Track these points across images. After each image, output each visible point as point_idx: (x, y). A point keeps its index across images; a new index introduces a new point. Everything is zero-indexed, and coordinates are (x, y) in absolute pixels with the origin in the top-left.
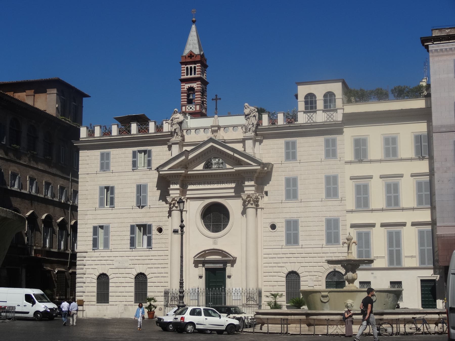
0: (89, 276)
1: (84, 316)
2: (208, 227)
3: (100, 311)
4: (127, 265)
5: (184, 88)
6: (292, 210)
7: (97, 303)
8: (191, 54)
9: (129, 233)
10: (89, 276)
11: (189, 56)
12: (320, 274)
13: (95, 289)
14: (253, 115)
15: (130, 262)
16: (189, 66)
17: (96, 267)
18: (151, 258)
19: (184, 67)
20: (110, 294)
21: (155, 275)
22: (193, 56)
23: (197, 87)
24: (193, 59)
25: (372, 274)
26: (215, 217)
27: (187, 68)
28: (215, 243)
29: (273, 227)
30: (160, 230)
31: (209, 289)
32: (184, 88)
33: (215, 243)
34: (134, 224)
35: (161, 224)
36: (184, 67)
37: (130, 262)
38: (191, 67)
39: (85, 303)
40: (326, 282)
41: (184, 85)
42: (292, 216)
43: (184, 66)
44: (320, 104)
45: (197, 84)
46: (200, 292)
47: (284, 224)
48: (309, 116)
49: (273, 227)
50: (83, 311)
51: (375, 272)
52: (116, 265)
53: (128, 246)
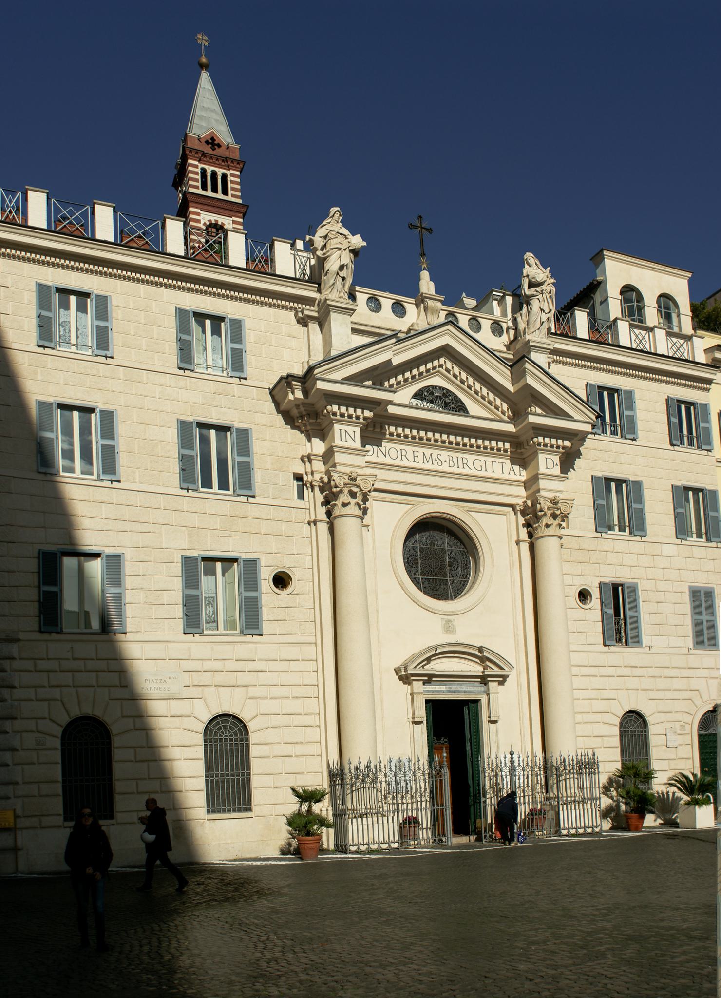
1: (22, 867)
8: (213, 139)
9: (177, 583)
11: (207, 142)
15: (186, 679)
16: (209, 169)
19: (197, 167)
20: (119, 786)
21: (276, 721)
22: (219, 146)
24: (218, 152)
26: (440, 556)
27: (204, 171)
28: (449, 628)
30: (281, 580)
33: (449, 628)
34: (195, 554)
35: (286, 564)
36: (197, 167)
37: (186, 679)
38: (214, 174)
40: (700, 736)
43: (196, 163)
46: (516, 764)
48: (637, 337)
53: (179, 625)
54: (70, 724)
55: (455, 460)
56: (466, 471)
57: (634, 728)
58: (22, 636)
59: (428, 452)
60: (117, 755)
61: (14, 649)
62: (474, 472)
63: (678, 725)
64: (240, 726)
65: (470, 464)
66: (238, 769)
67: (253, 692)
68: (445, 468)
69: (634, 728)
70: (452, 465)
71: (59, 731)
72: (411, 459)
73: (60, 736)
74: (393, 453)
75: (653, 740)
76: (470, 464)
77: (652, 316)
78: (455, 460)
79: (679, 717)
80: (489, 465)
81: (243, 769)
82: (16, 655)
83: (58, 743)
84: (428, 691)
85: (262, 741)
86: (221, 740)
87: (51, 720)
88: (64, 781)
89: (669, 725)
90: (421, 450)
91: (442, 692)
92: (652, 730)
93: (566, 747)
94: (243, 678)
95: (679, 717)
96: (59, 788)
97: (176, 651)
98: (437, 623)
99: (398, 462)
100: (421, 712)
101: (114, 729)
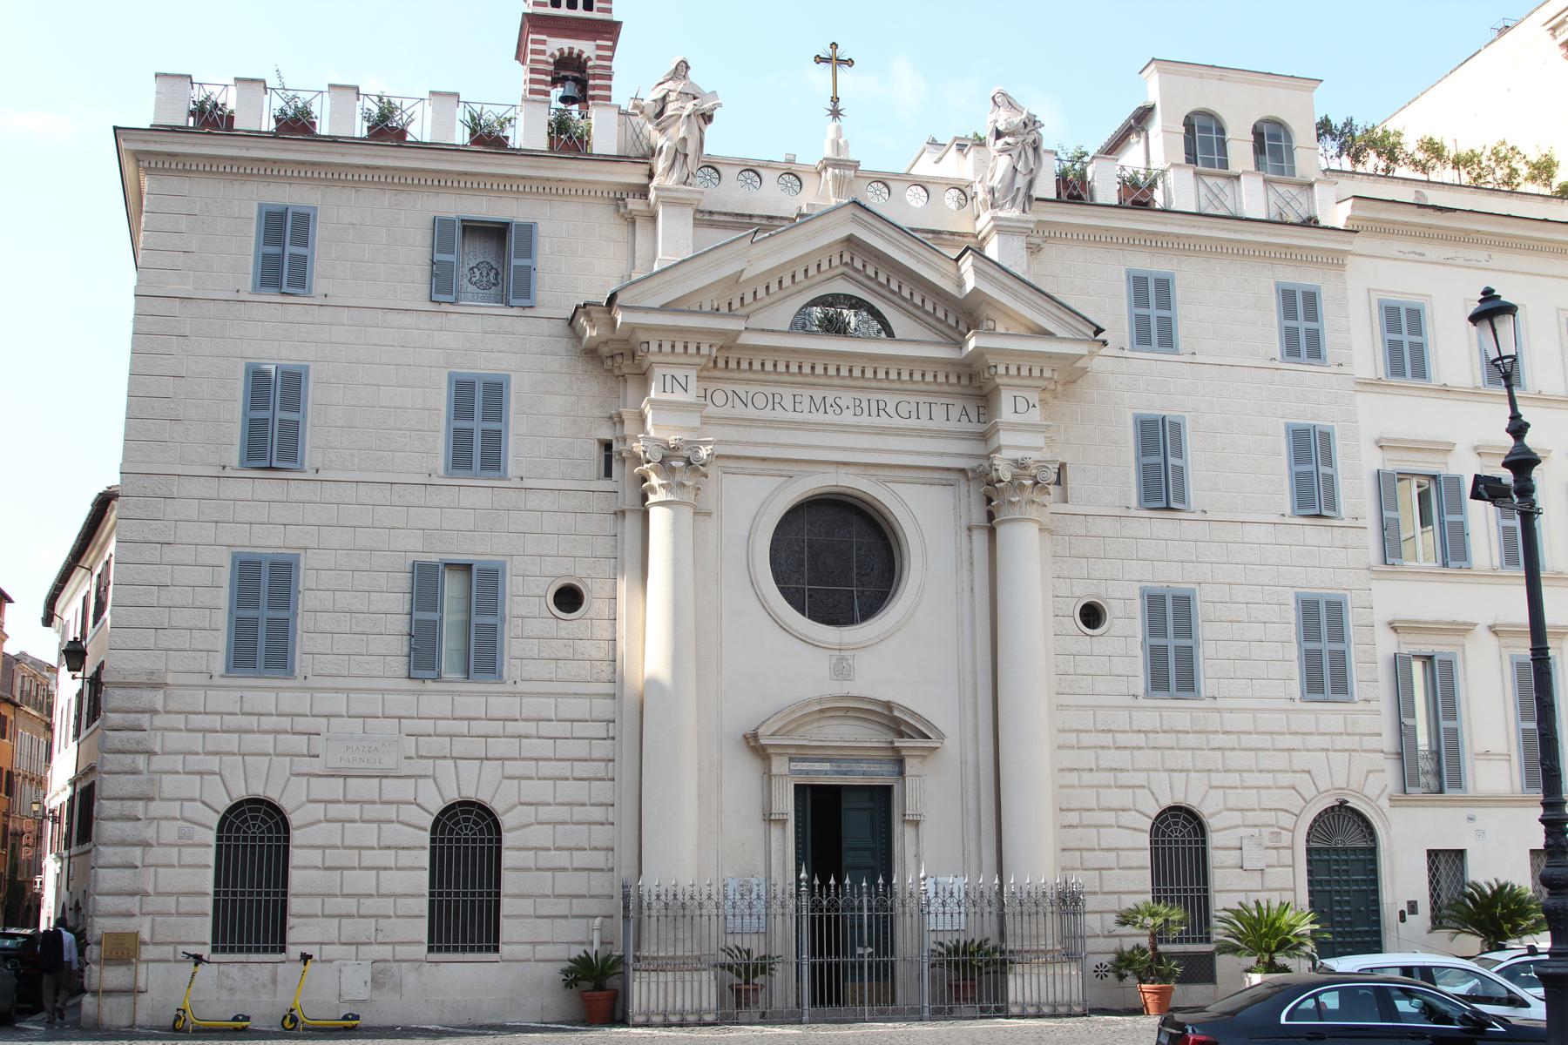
0: (174, 809)
2: (794, 598)
3: (231, 990)
4: (389, 762)
5: (543, 52)
6: (1155, 554)
7: (214, 950)
10: (174, 809)
12: (1286, 820)
13: (207, 880)
14: (1030, 139)
15: (409, 745)
17: (213, 763)
18: (522, 728)
20: (294, 905)
23: (599, 57)
25: (1471, 819)
26: (837, 558)
28: (842, 671)
29: (1092, 615)
31: (824, 881)
32: (543, 52)
33: (842, 671)
37: (409, 745)
39: (147, 952)
40: (1309, 851)
41: (543, 42)
42: (1170, 577)
44: (1240, 153)
45: (599, 47)
47: (1137, 607)
49: (1092, 615)
50: (133, 991)
51: (1478, 812)
52: (334, 757)
54: (231, 810)
55: (865, 405)
56: (884, 421)
57: (1180, 840)
58: (170, 679)
59: (818, 395)
60: (296, 857)
61: (157, 699)
62: (897, 422)
63: (1266, 832)
64: (489, 820)
65: (891, 409)
66: (481, 887)
67: (513, 768)
68: (847, 417)
69: (1180, 840)
70: (858, 411)
71: (214, 820)
72: (789, 406)
73: (215, 827)
74: (760, 401)
75: (1215, 857)
76: (891, 409)
77: (1240, 153)
78: (865, 405)
79: (1269, 817)
80: (924, 410)
81: (489, 886)
82: (160, 707)
83: (211, 837)
84: (801, 772)
85: (520, 843)
86: (458, 841)
87: (203, 803)
88: (216, 893)
89: (1244, 831)
90: (807, 392)
91: (824, 774)
92: (1214, 839)
93: (1038, 865)
94: (499, 747)
95: (1269, 817)
96: (208, 904)
97: (397, 704)
98: (821, 663)
99: (767, 414)
100: (786, 804)
101: (294, 819)
